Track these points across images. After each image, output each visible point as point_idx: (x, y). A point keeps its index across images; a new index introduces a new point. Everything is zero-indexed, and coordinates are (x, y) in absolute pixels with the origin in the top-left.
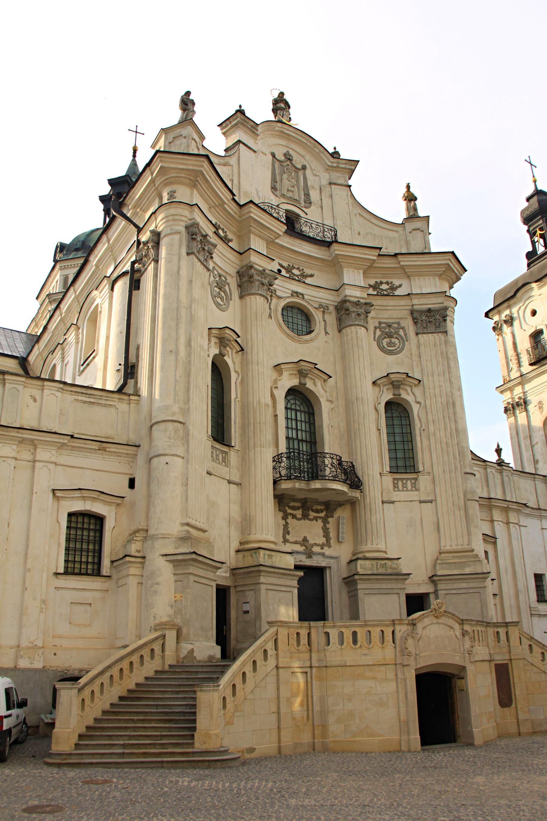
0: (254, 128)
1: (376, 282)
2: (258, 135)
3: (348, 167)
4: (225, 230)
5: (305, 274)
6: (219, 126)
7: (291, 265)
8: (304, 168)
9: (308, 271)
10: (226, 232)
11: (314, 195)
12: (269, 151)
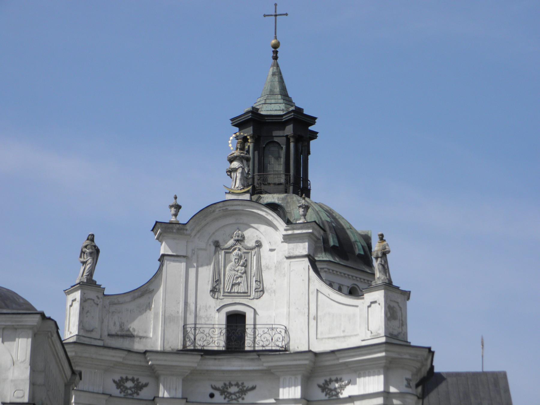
0: (181, 229)
1: (326, 381)
2: (190, 235)
3: (304, 231)
4: (136, 378)
5: (245, 389)
6: (152, 230)
7: (227, 383)
8: (259, 245)
9: (249, 384)
10: (138, 380)
11: (268, 278)
12: (210, 242)
